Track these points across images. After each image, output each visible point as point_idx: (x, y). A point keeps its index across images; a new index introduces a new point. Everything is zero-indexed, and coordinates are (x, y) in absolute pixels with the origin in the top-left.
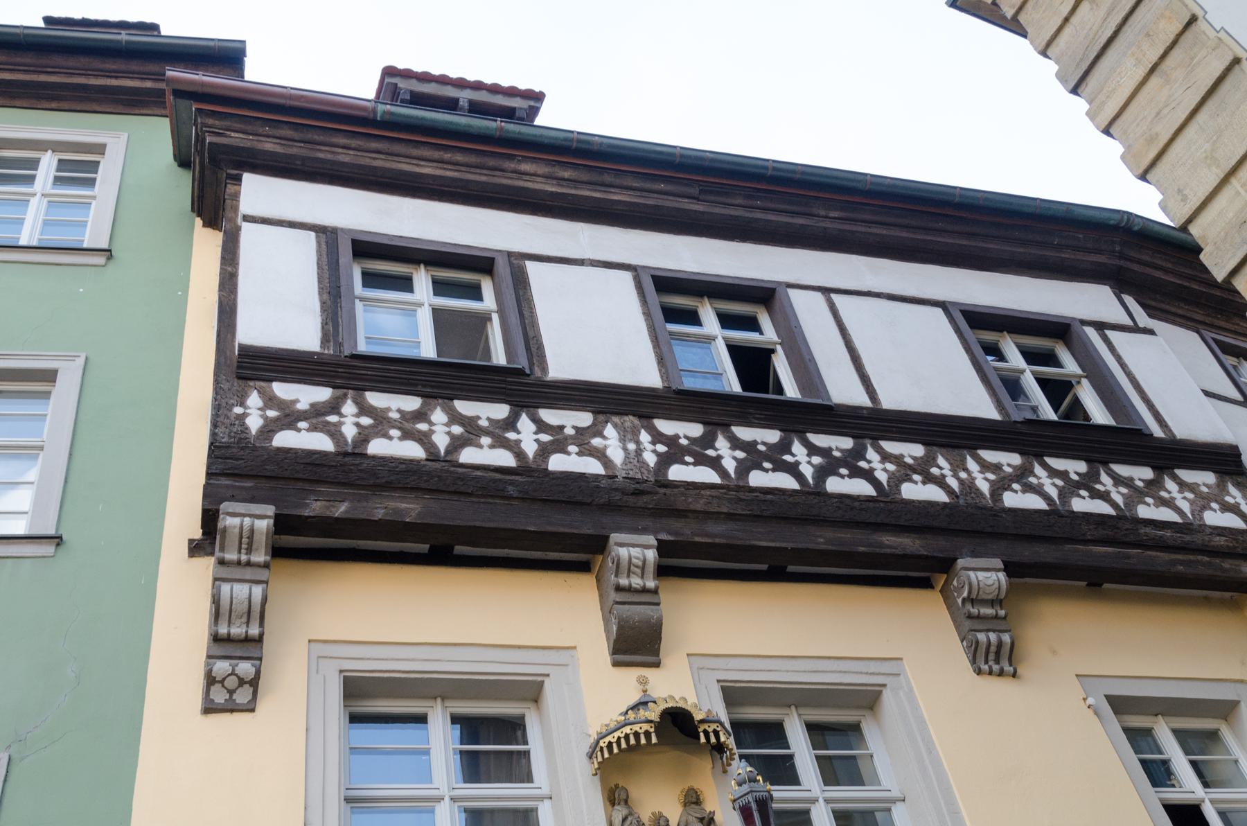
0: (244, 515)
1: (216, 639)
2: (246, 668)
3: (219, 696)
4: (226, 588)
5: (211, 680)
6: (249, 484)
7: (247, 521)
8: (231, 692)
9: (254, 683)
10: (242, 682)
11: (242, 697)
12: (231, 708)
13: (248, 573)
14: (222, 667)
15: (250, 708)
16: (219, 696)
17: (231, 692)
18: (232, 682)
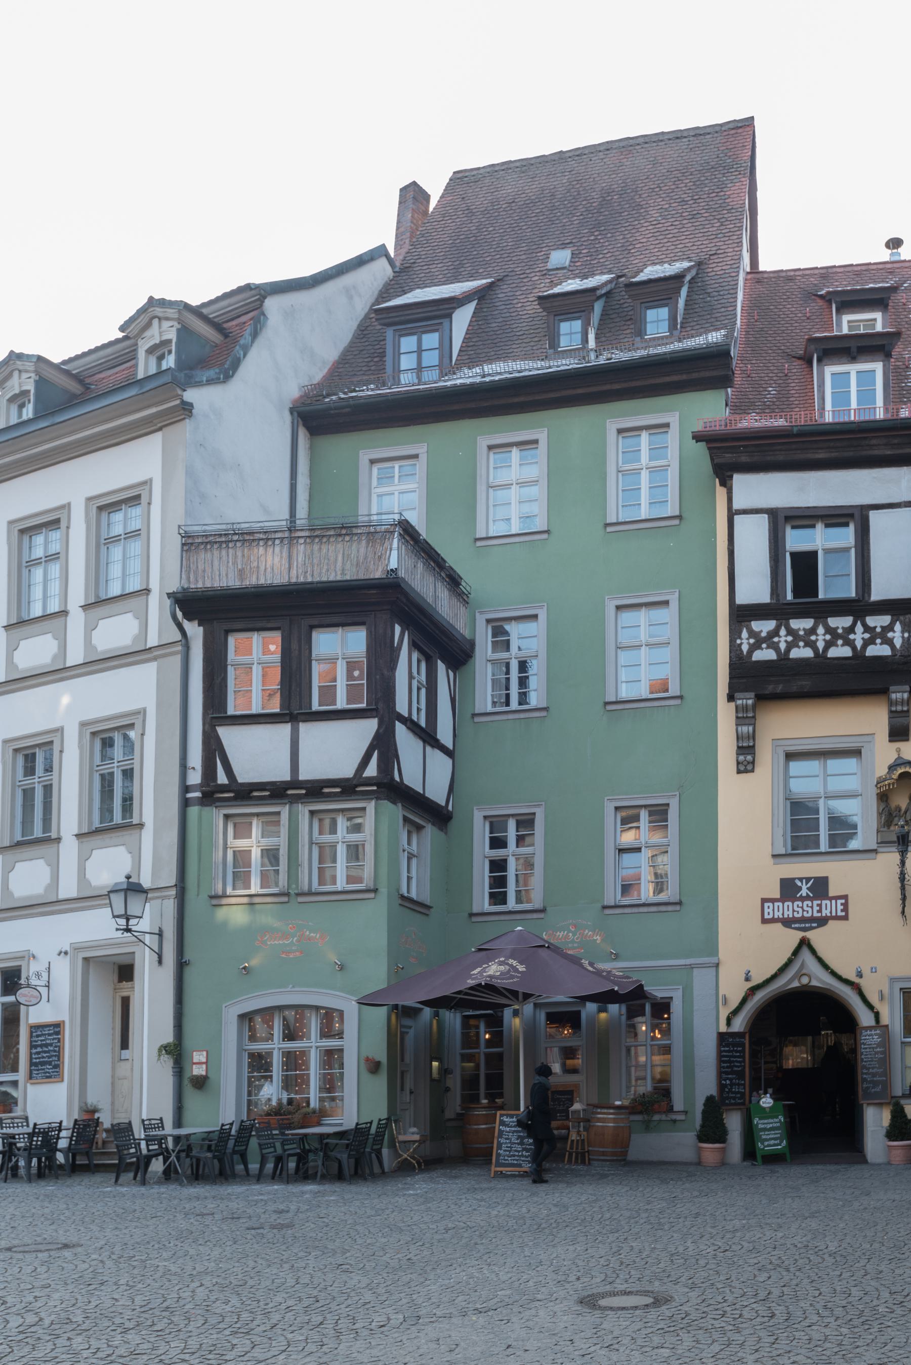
0: (743, 699)
1: (739, 747)
2: (749, 758)
3: (742, 768)
4: (740, 728)
5: (738, 763)
6: (744, 680)
7: (745, 701)
8: (746, 766)
9: (753, 763)
10: (749, 763)
11: (749, 767)
12: (746, 771)
13: (747, 721)
14: (741, 758)
15: (752, 771)
16: (742, 768)
17: (746, 766)
18: (745, 763)
